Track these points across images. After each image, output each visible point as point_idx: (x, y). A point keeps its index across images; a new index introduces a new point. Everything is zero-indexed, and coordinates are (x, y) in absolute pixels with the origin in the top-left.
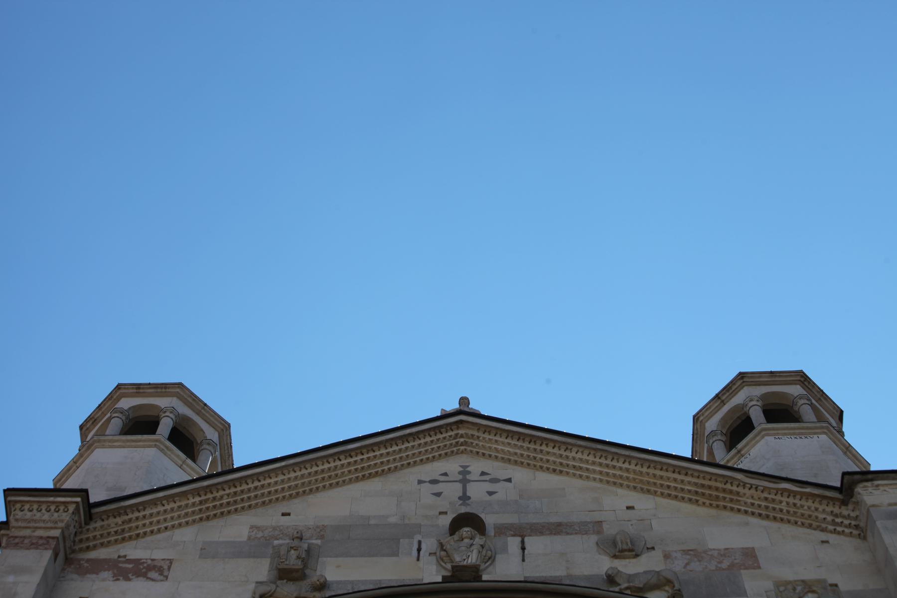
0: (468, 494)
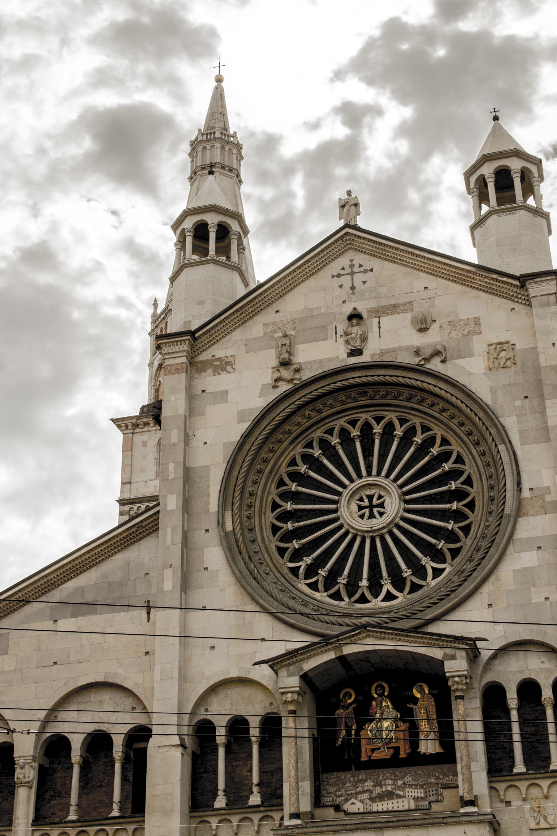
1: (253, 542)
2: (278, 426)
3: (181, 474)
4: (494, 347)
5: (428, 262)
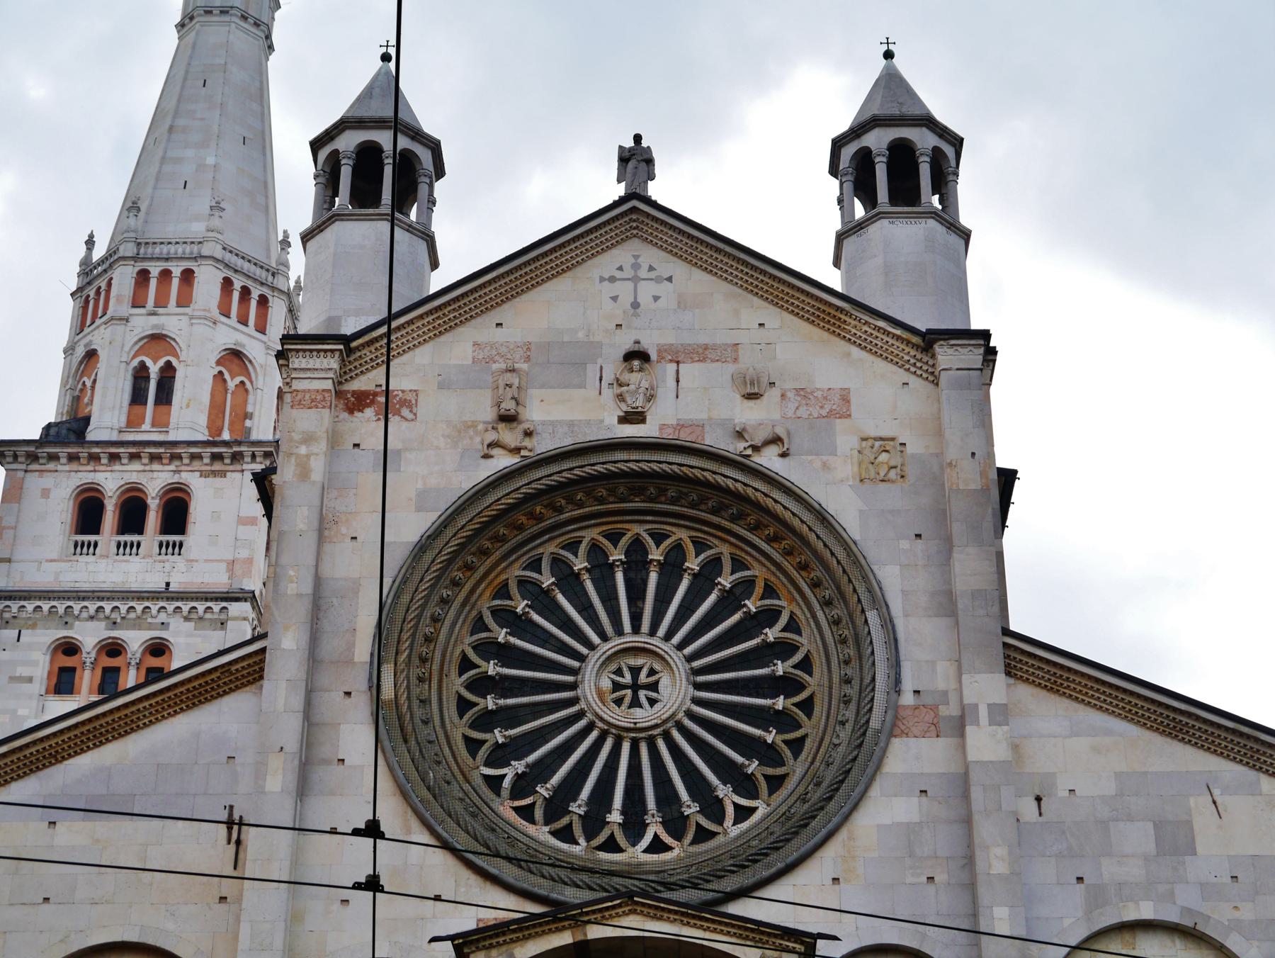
0: (638, 300)
1: (425, 722)
2: (486, 525)
3: (307, 588)
4: (870, 442)
5: (771, 282)
